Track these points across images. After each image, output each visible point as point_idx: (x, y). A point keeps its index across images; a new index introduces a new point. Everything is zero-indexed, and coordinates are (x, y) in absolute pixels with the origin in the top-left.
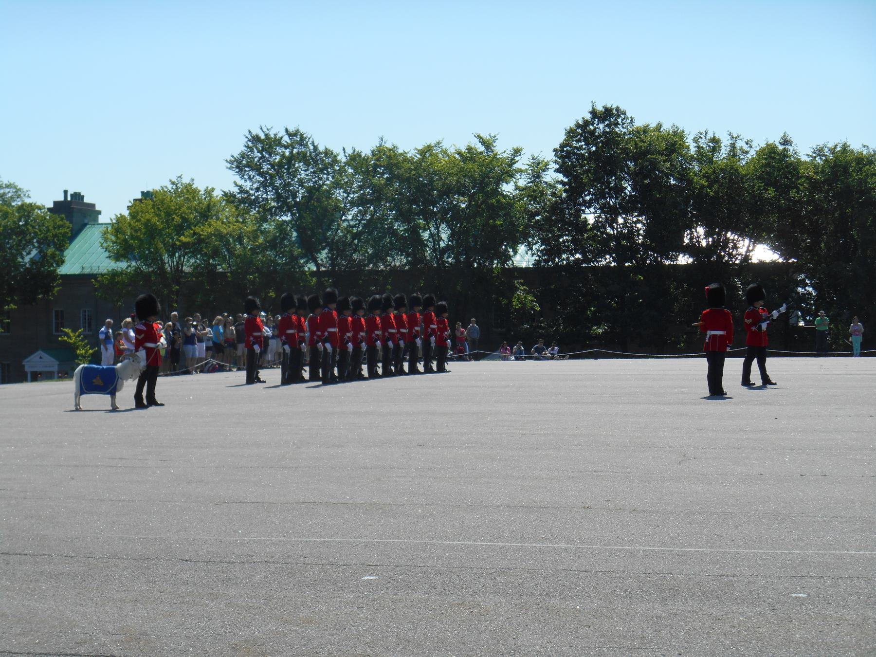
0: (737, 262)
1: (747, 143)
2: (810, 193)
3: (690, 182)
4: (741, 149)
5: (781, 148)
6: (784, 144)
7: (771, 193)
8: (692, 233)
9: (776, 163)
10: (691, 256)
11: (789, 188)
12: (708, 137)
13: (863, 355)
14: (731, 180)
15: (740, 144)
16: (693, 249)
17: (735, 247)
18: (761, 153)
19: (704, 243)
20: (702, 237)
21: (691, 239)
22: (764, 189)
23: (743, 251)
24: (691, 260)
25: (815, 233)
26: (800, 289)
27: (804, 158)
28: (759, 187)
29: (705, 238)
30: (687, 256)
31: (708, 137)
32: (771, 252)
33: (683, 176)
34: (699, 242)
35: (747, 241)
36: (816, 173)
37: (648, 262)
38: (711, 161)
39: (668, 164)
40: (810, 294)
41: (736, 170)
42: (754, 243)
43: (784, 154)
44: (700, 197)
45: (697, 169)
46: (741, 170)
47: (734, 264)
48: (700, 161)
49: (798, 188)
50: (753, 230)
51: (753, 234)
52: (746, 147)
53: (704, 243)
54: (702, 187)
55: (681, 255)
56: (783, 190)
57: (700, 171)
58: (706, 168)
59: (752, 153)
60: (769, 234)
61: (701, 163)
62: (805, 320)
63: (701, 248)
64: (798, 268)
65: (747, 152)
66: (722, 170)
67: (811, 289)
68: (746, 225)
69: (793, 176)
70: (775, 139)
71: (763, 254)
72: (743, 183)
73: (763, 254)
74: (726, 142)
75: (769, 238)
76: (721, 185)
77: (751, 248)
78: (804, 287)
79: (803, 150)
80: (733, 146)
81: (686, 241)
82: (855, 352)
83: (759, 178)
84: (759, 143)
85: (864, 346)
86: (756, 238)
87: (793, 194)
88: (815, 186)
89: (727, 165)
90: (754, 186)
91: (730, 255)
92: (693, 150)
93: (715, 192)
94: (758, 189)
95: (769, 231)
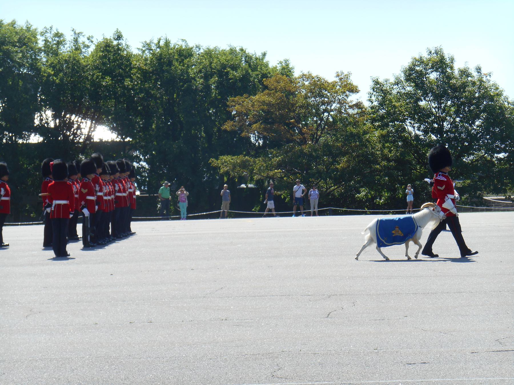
0: (81, 140)
1: (89, 39)
2: (142, 82)
3: (38, 70)
4: (84, 43)
5: (115, 43)
6: (117, 39)
7: (107, 81)
8: (41, 115)
9: (112, 56)
10: (41, 135)
11: (123, 78)
12: (53, 32)
13: (188, 218)
14: (73, 69)
15: (81, 40)
16: (42, 130)
17: (79, 128)
18: (98, 47)
19: (52, 125)
20: (50, 119)
21: (41, 120)
22: (102, 78)
23: (85, 131)
24: (41, 139)
25: (147, 115)
26: (135, 164)
27: (135, 51)
28: (98, 76)
29: (53, 120)
30: (38, 136)
31: (53, 32)
32: (110, 132)
33: (33, 67)
34: (47, 123)
35: (89, 122)
36: (146, 65)
37: (4, 141)
38: (56, 53)
39: (20, 55)
40: (143, 167)
41: (78, 61)
42: (95, 124)
43: (118, 49)
44: (47, 85)
45: (44, 60)
46: (82, 61)
47: (78, 142)
48: (47, 53)
49: (131, 78)
50: (94, 113)
51: (94, 116)
52: (87, 43)
53: (52, 125)
54: (49, 75)
55: (33, 135)
56: (119, 79)
57: (47, 61)
58: (52, 59)
59: (92, 48)
60: (107, 117)
61: (48, 55)
62: (140, 189)
63: (49, 129)
64: (133, 146)
65: (88, 47)
66: (66, 60)
67: (144, 164)
68: (88, 109)
69: (126, 66)
70: (110, 35)
71: (104, 134)
72: (84, 72)
73: (104, 134)
74: (69, 37)
75: (108, 120)
76: (65, 74)
77: (92, 129)
78: (138, 163)
79: (134, 44)
80: (76, 40)
81: (37, 122)
82: (182, 216)
83: (96, 68)
84: (98, 38)
85: (189, 211)
86: (98, 120)
87: (127, 82)
88: (145, 75)
89: (70, 57)
90: (93, 75)
91: (75, 134)
92: (41, 44)
93: (61, 80)
94: (97, 78)
95: (107, 113)
